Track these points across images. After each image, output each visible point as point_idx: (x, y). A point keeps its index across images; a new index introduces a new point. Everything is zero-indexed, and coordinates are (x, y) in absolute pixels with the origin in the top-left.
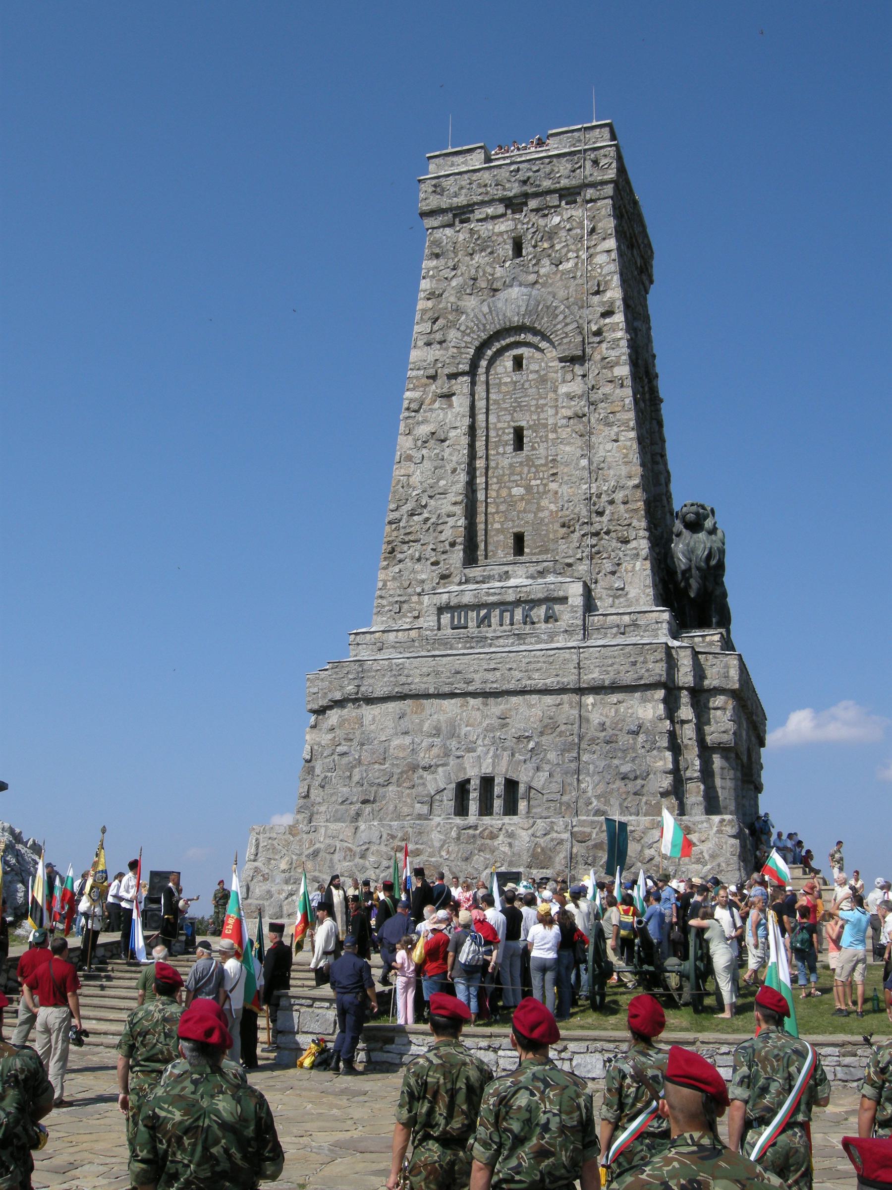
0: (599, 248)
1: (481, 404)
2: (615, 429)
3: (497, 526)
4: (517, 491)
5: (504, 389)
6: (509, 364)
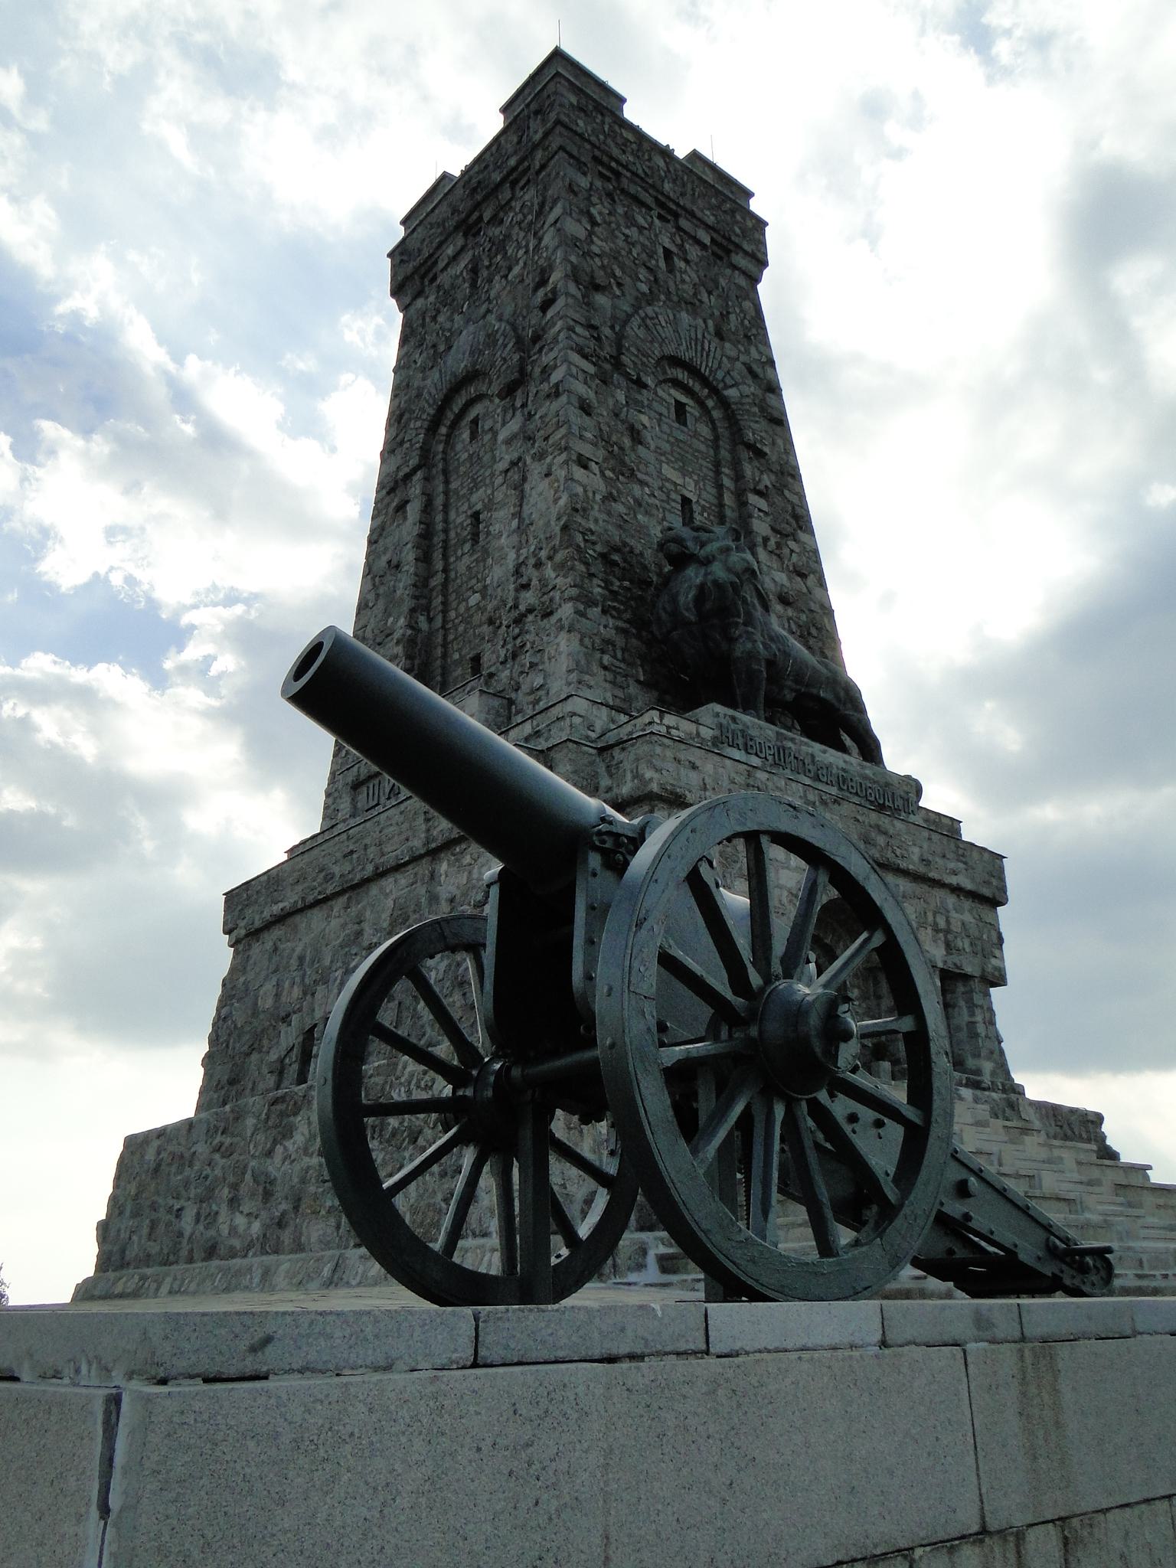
0: (546, 226)
1: (439, 500)
2: (548, 460)
3: (456, 656)
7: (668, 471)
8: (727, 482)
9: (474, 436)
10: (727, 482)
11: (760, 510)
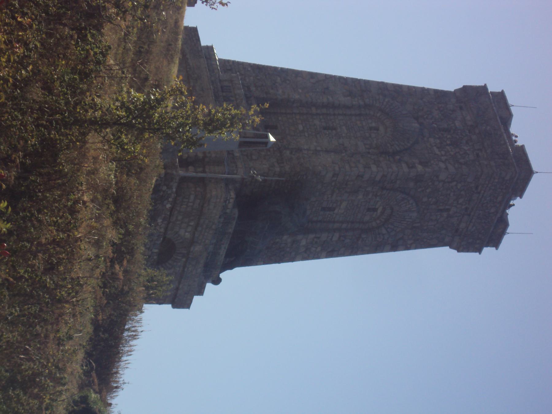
3: (280, 118)
4: (301, 127)
5: (358, 122)
6: (374, 125)
7: (344, 205)
8: (344, 226)
9: (371, 129)
10: (344, 226)
11: (332, 237)
